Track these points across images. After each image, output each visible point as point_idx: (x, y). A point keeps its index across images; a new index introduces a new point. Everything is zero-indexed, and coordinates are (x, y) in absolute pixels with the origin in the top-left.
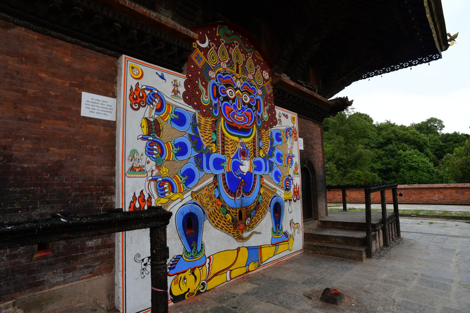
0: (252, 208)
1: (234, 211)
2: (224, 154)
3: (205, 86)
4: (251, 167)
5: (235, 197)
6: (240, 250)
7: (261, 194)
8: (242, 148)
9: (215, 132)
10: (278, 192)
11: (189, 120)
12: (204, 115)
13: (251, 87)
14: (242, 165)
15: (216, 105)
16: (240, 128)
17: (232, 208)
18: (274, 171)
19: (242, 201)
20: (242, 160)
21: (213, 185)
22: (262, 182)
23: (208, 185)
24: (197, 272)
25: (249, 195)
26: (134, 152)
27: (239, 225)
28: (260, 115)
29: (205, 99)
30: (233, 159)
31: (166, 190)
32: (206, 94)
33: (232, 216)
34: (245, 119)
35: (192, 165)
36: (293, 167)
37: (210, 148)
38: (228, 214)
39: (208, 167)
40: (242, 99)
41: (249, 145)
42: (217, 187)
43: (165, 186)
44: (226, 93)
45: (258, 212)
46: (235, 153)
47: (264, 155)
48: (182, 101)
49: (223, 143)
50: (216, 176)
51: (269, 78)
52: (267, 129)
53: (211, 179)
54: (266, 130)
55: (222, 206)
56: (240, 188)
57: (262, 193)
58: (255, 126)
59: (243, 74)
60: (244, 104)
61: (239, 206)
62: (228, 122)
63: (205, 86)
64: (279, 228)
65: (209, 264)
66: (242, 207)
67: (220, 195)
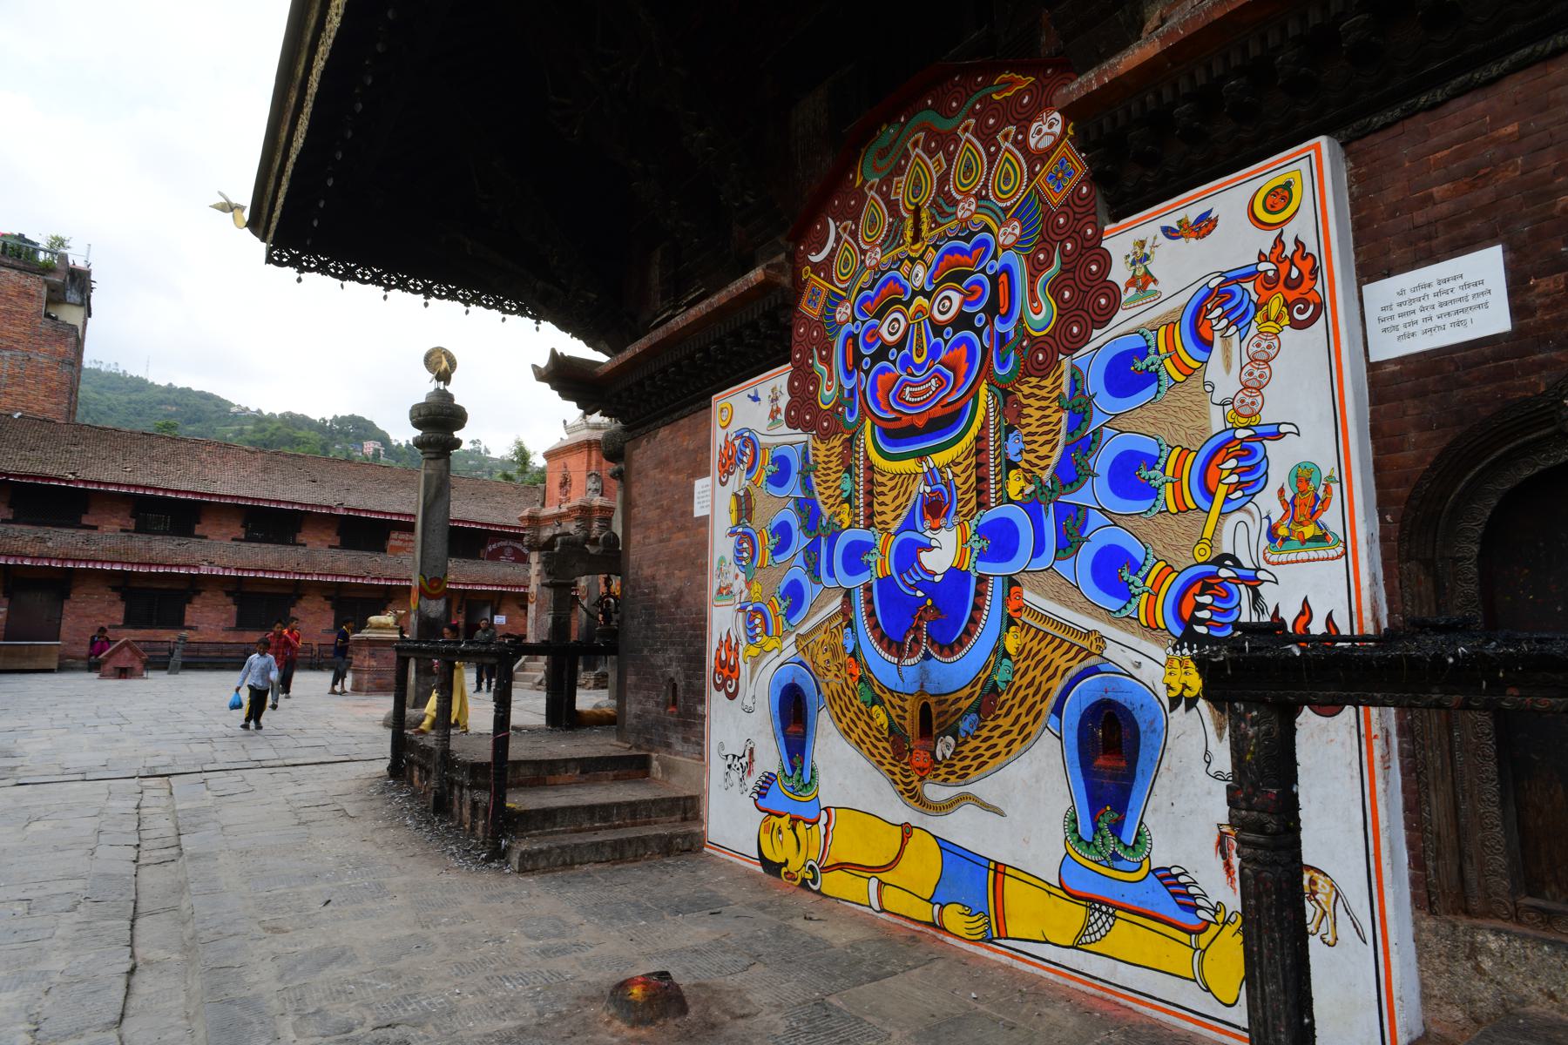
0: (964, 704)
1: (896, 701)
2: (872, 525)
3: (827, 361)
4: (963, 551)
5: (900, 657)
6: (910, 835)
7: (1006, 655)
8: (928, 489)
9: (849, 470)
10: (1111, 652)
11: (796, 466)
12: (824, 436)
13: (968, 246)
14: (929, 548)
15: (852, 392)
16: (920, 423)
17: (891, 691)
18: (1087, 553)
19: (924, 675)
20: (928, 533)
21: (840, 619)
22: (1013, 605)
23: (830, 619)
24: (801, 827)
25: (953, 653)
26: (722, 560)
27: (911, 750)
28: (1009, 328)
29: (827, 394)
30: (896, 534)
31: (758, 630)
32: (831, 378)
33: (888, 715)
34: (943, 380)
35: (800, 573)
36: (1269, 503)
37: (836, 520)
38: (876, 708)
39: (831, 573)
40: (931, 319)
41: (958, 470)
42: (850, 624)
43: (757, 621)
44: (880, 337)
45: (992, 724)
46: (905, 513)
47: (1029, 489)
48: (785, 429)
49: (869, 493)
50: (848, 594)
51: (1065, 126)
52: (1043, 371)
53: (836, 603)
54: (1044, 377)
55: (861, 679)
56: (919, 628)
57: (1011, 650)
58: (983, 389)
59: (939, 225)
60: (938, 329)
61: (915, 688)
62: (884, 425)
63: (827, 361)
64: (1116, 829)
65: (826, 825)
66: (922, 692)
67: (858, 645)
